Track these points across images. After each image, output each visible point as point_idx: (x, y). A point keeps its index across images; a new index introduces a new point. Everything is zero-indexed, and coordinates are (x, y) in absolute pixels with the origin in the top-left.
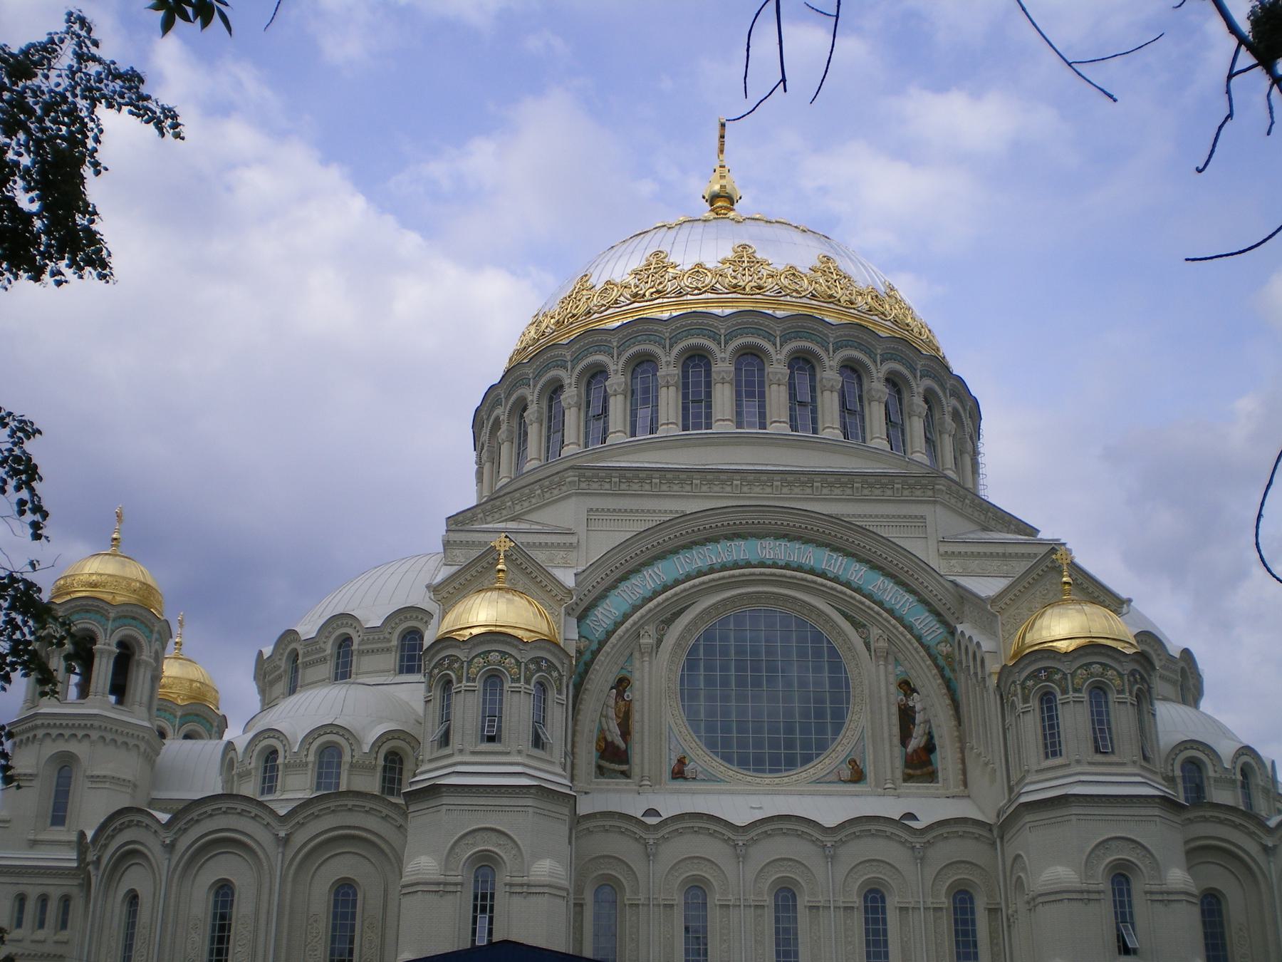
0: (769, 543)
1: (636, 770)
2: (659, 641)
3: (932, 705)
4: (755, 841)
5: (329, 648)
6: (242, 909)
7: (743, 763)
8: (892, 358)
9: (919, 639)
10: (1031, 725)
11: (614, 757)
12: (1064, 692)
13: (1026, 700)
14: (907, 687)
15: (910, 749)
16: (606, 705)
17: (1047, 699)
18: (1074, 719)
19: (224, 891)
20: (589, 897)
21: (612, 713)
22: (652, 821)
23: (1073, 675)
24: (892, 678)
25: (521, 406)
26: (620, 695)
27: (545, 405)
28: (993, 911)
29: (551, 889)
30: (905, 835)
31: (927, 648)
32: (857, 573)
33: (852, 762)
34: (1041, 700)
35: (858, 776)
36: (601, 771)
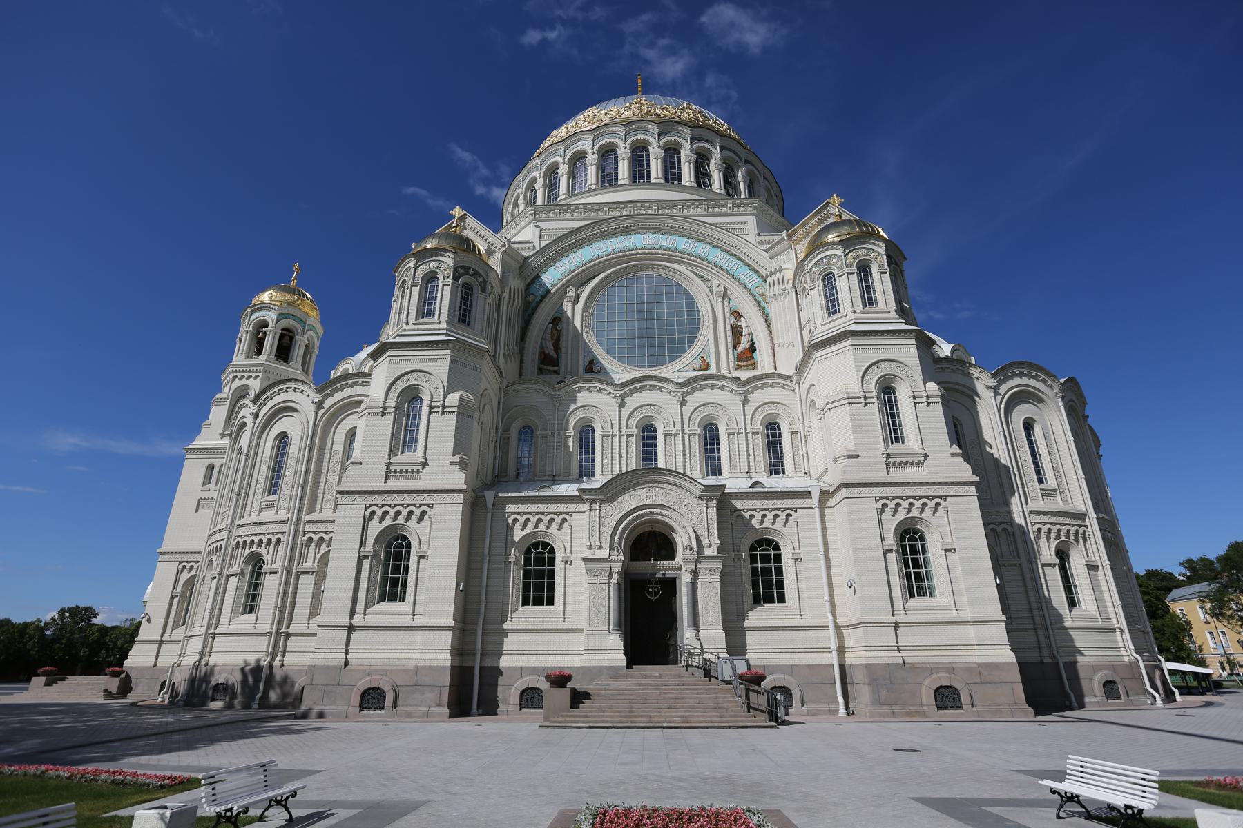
0: (650, 235)
1: (563, 369)
6: (294, 448)
8: (728, 149)
10: (815, 299)
12: (840, 268)
13: (813, 281)
14: (737, 315)
15: (739, 350)
16: (545, 333)
19: (283, 438)
21: (548, 337)
24: (727, 309)
26: (555, 327)
32: (702, 249)
34: (823, 280)
36: (541, 371)
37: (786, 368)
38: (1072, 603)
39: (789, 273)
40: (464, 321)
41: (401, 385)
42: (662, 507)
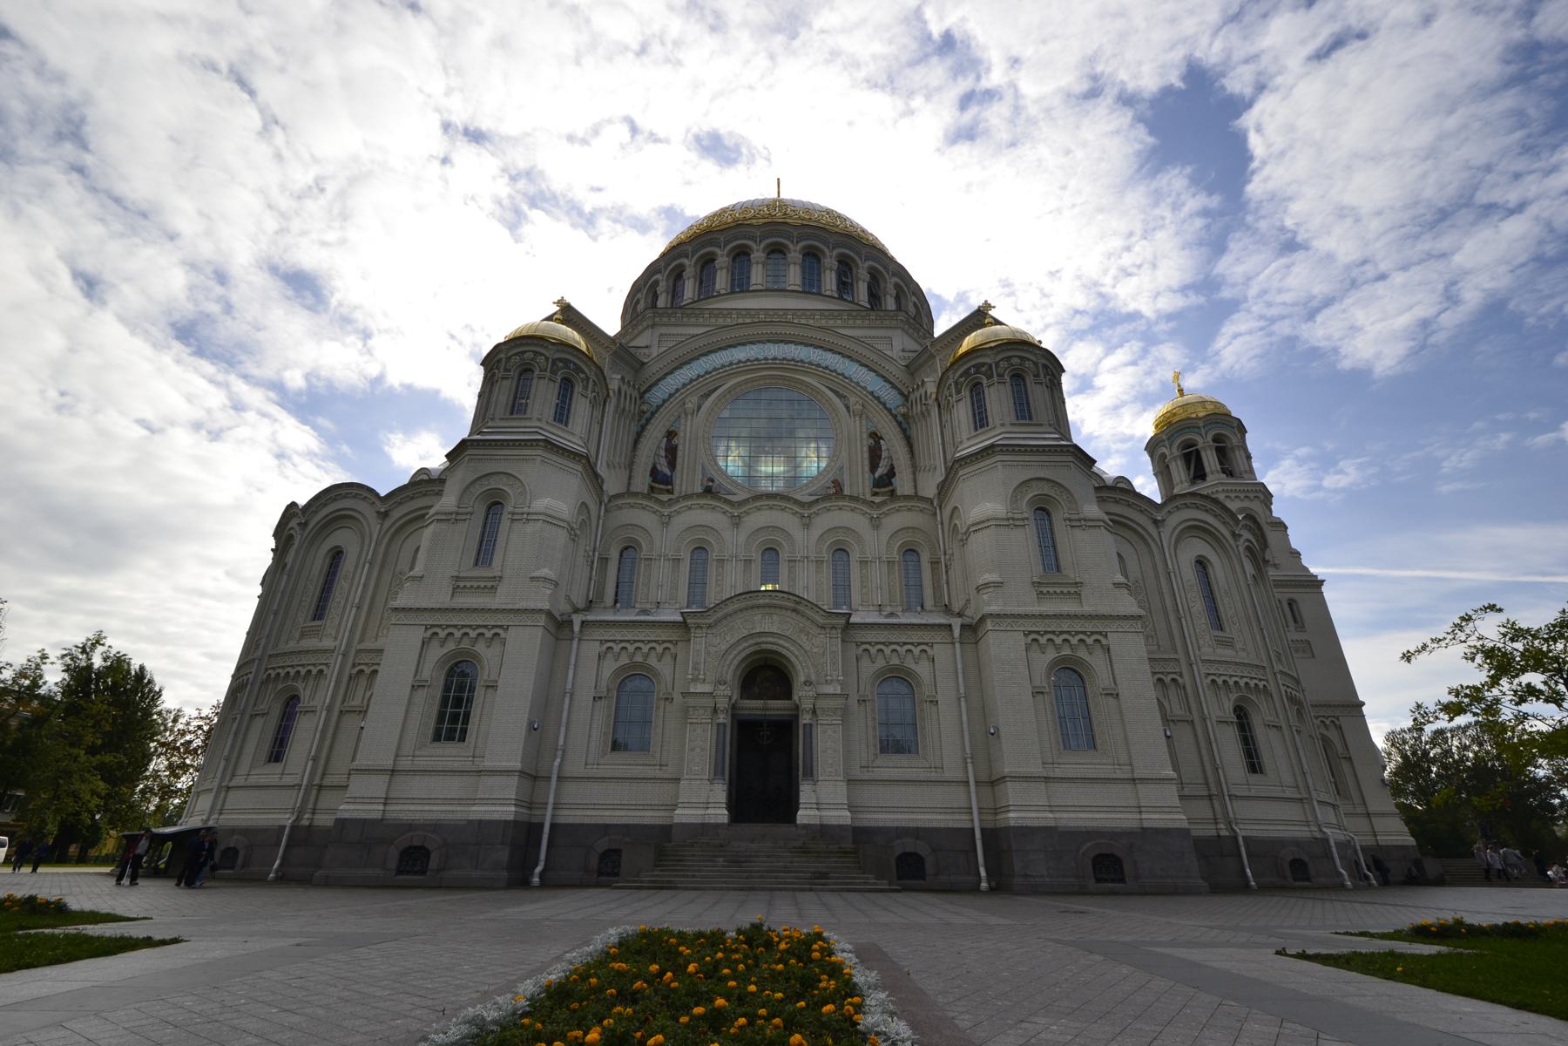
1: (677, 488)
2: (699, 408)
3: (893, 444)
4: (747, 513)
6: (348, 564)
9: (884, 404)
10: (962, 412)
12: (990, 377)
13: (958, 392)
14: (875, 436)
17: (976, 389)
18: (998, 399)
20: (614, 554)
23: (997, 364)
26: (669, 441)
28: (935, 563)
29: (550, 519)
31: (889, 410)
37: (929, 489)
38: (1254, 766)
39: (931, 388)
40: (560, 421)
41: (479, 489)
42: (781, 636)
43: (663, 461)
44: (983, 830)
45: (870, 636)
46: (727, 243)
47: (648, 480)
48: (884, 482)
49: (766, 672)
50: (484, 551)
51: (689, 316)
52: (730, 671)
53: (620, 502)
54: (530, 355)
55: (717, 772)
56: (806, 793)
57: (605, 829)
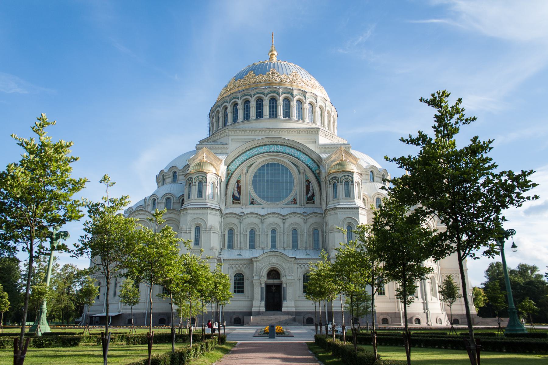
1: (241, 202)
2: (247, 171)
5: (171, 175)
7: (267, 200)
11: (236, 199)
12: (338, 182)
13: (330, 185)
14: (308, 181)
20: (227, 233)
22: (242, 214)
25: (218, 112)
26: (238, 184)
27: (223, 112)
30: (302, 217)
33: (294, 199)
35: (296, 203)
36: (233, 203)
43: (236, 192)
44: (328, 312)
45: (302, 262)
46: (254, 95)
47: (232, 198)
48: (310, 199)
49: (274, 273)
50: (197, 242)
51: (242, 132)
52: (265, 273)
53: (227, 216)
54: (201, 177)
55: (262, 300)
56: (285, 304)
57: (234, 313)
